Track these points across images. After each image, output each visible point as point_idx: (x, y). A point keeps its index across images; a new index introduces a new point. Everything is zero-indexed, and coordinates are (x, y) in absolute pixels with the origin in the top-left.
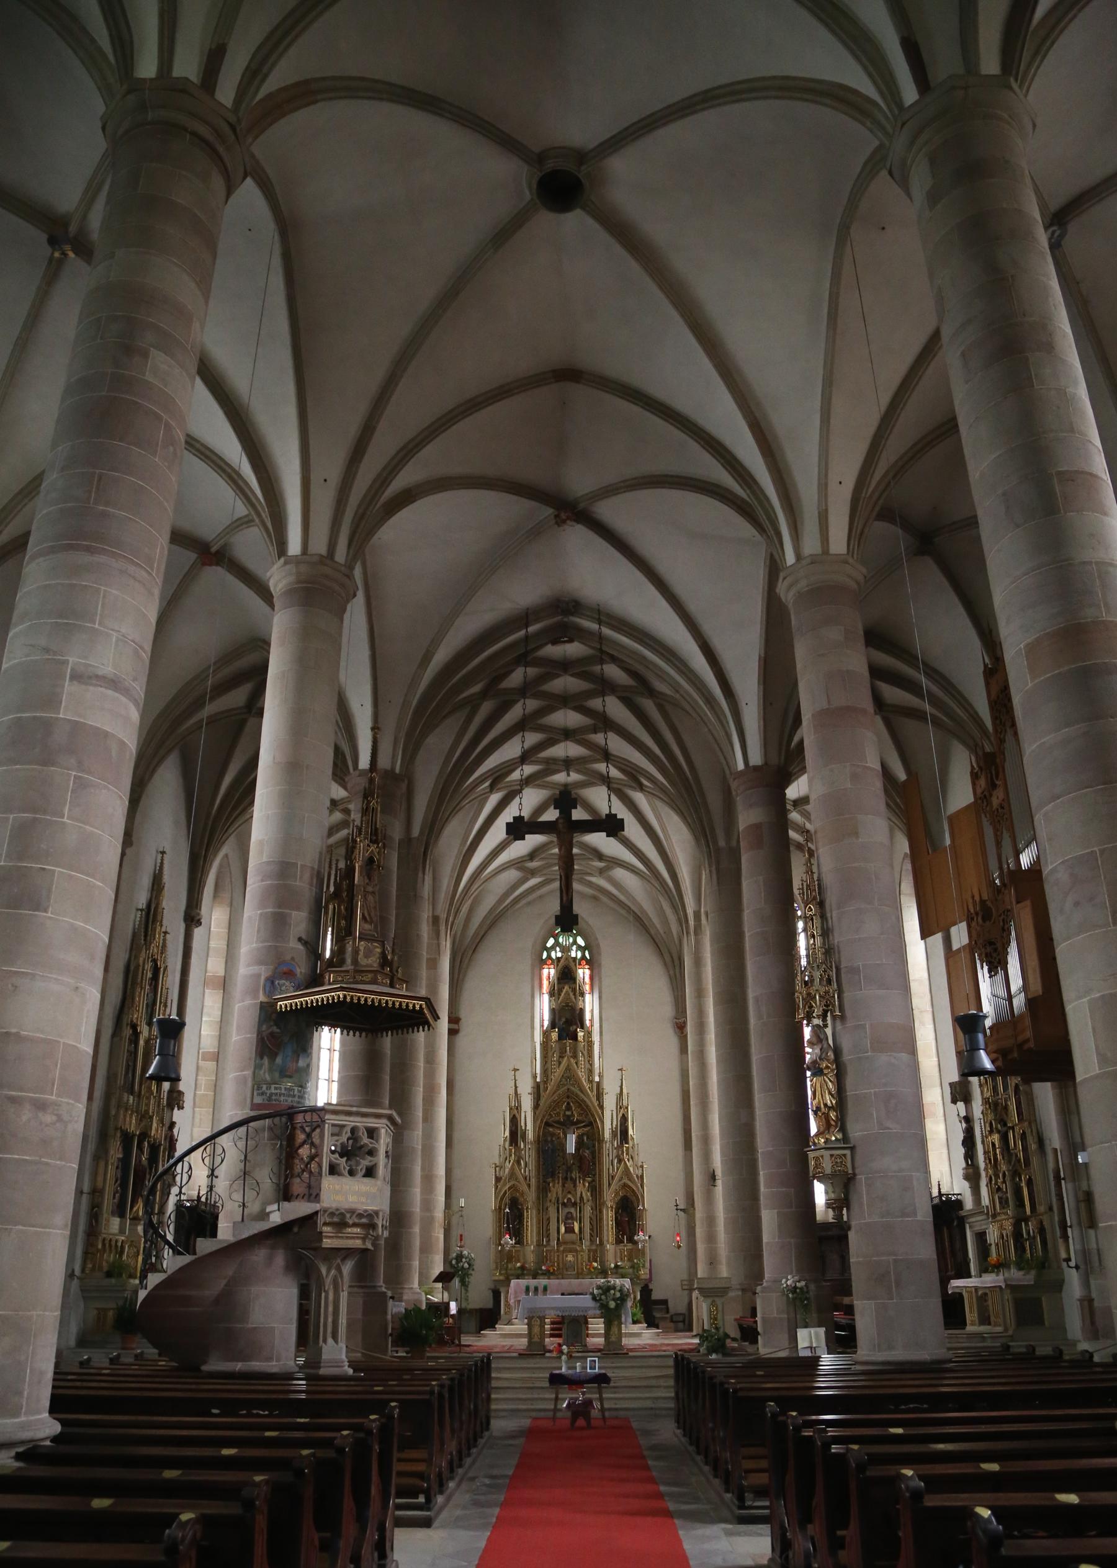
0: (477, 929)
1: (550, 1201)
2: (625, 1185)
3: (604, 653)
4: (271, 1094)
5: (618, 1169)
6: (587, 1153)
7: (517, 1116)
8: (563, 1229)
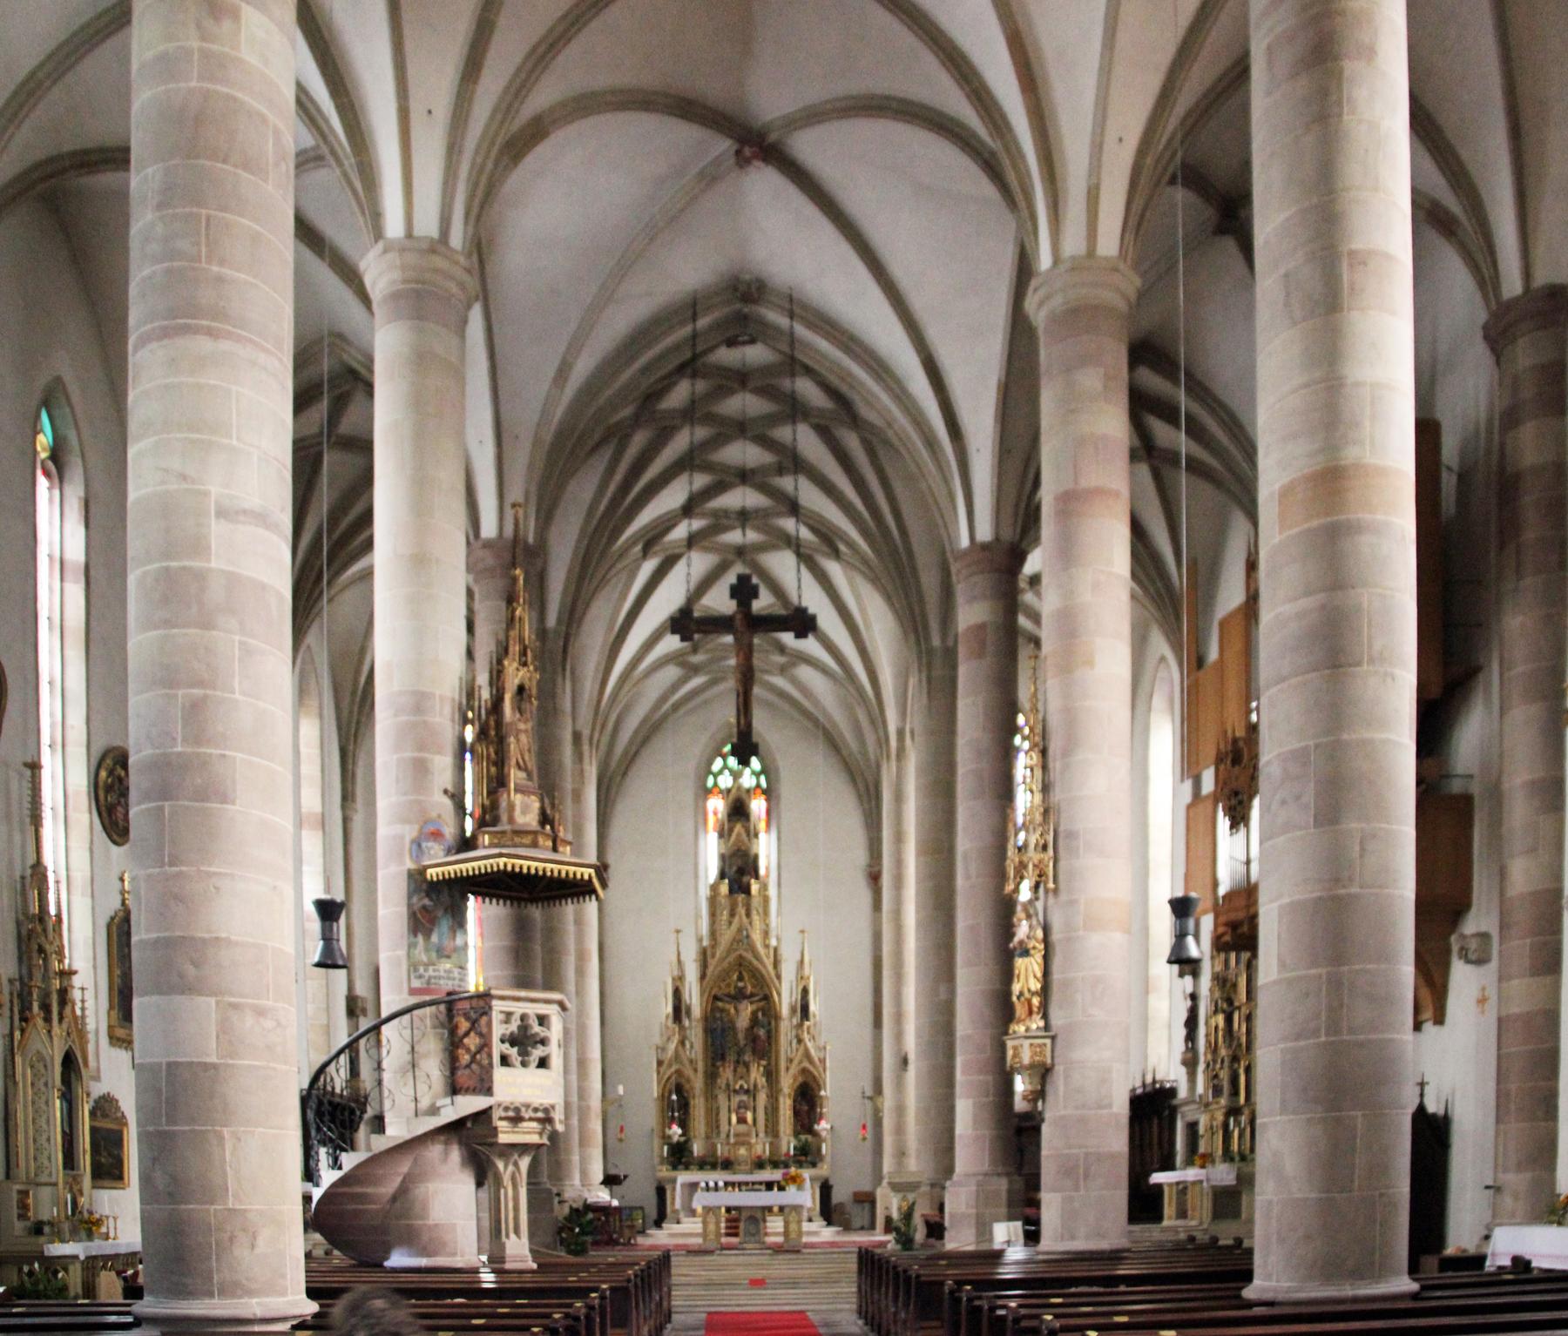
2: (804, 1071)
3: (793, 364)
4: (430, 978)
6: (762, 1032)
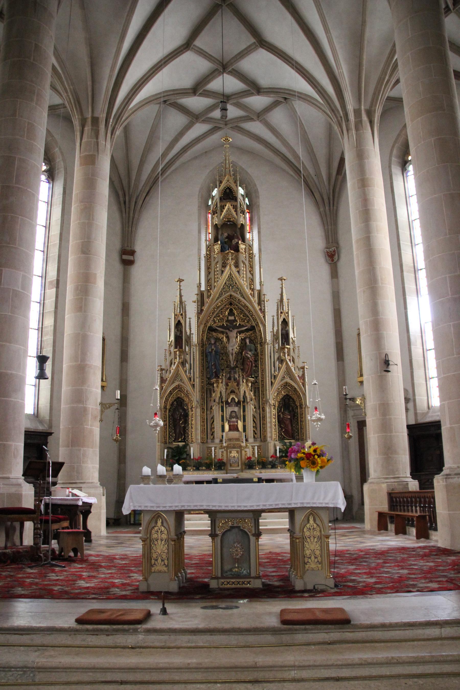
0: (150, 174)
1: (214, 401)
2: (286, 385)
5: (279, 369)
6: (249, 354)
7: (182, 322)
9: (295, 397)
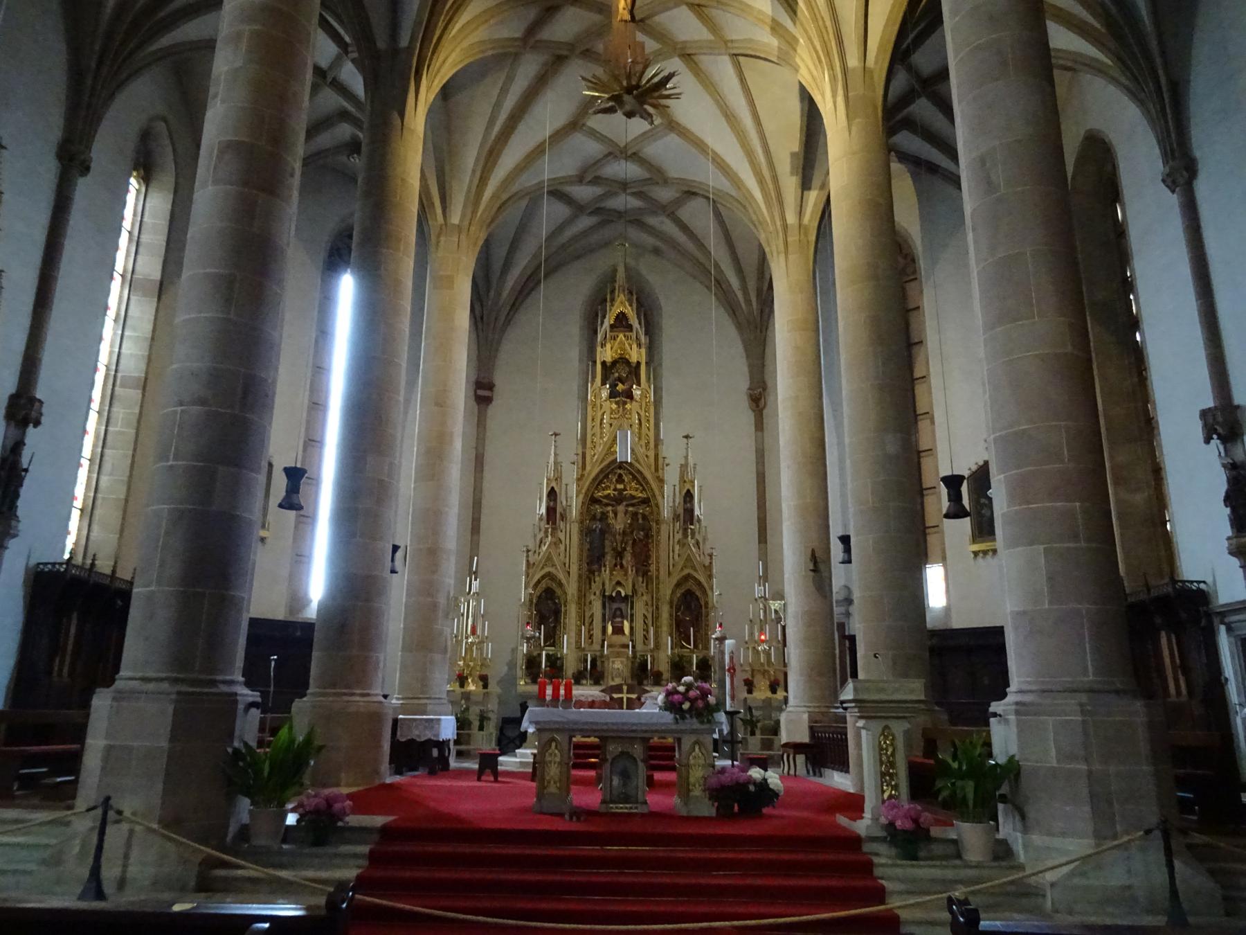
1: (595, 594)
8: (610, 629)
9: (698, 593)
